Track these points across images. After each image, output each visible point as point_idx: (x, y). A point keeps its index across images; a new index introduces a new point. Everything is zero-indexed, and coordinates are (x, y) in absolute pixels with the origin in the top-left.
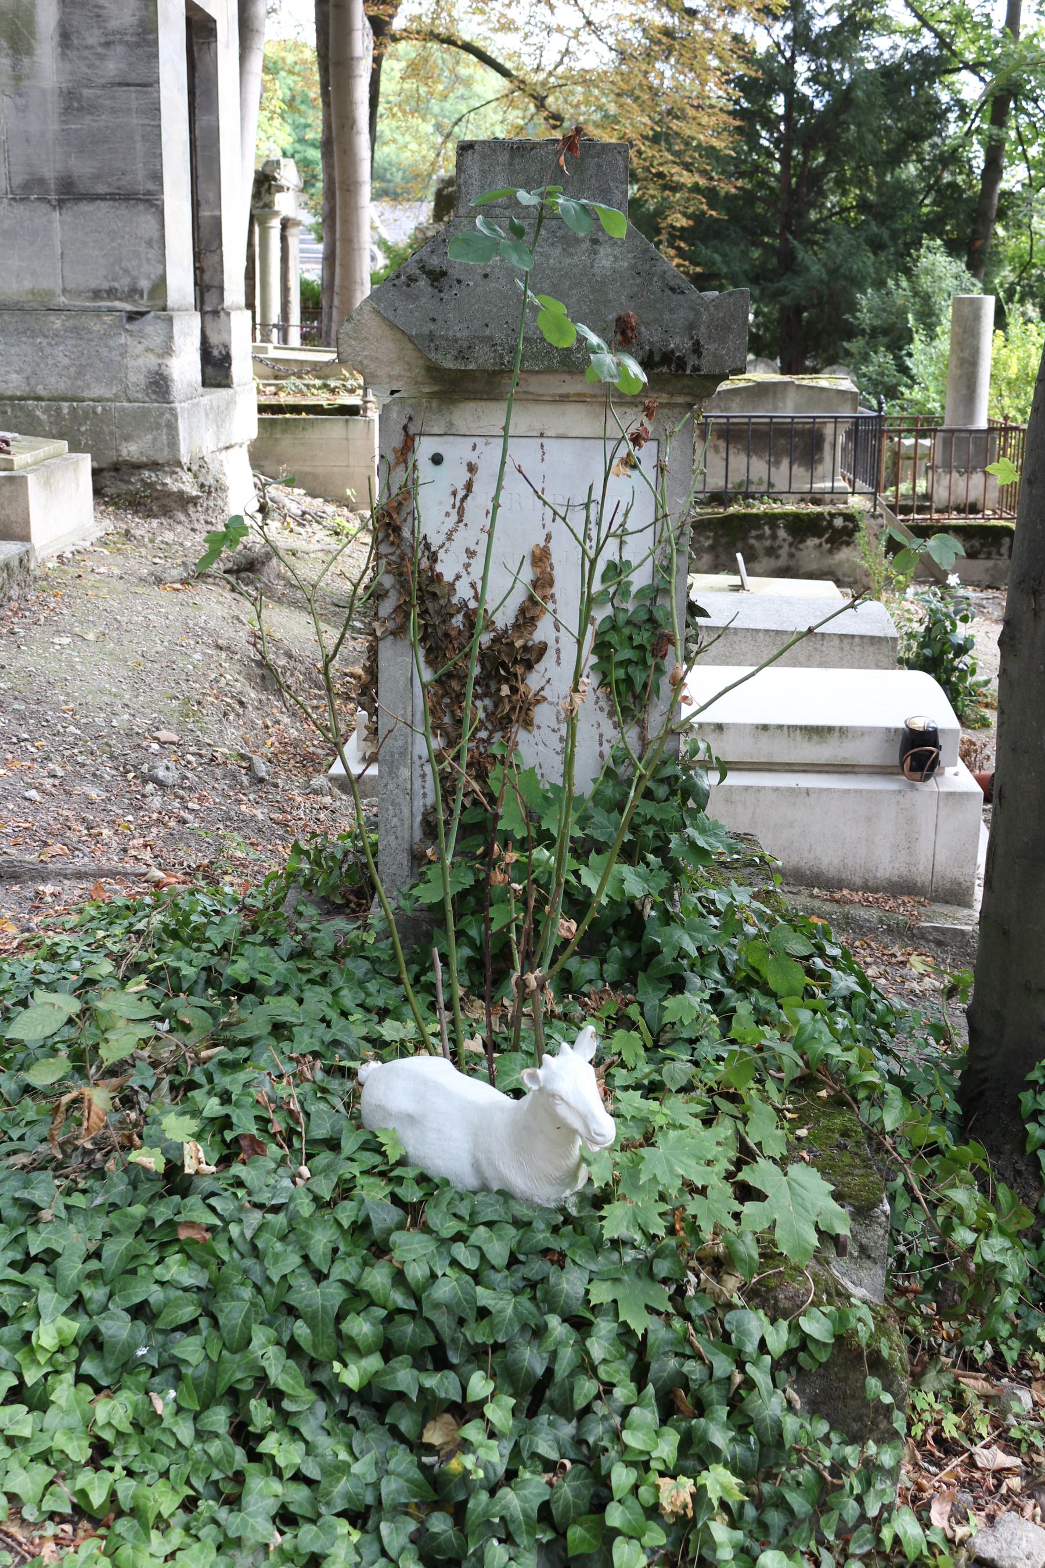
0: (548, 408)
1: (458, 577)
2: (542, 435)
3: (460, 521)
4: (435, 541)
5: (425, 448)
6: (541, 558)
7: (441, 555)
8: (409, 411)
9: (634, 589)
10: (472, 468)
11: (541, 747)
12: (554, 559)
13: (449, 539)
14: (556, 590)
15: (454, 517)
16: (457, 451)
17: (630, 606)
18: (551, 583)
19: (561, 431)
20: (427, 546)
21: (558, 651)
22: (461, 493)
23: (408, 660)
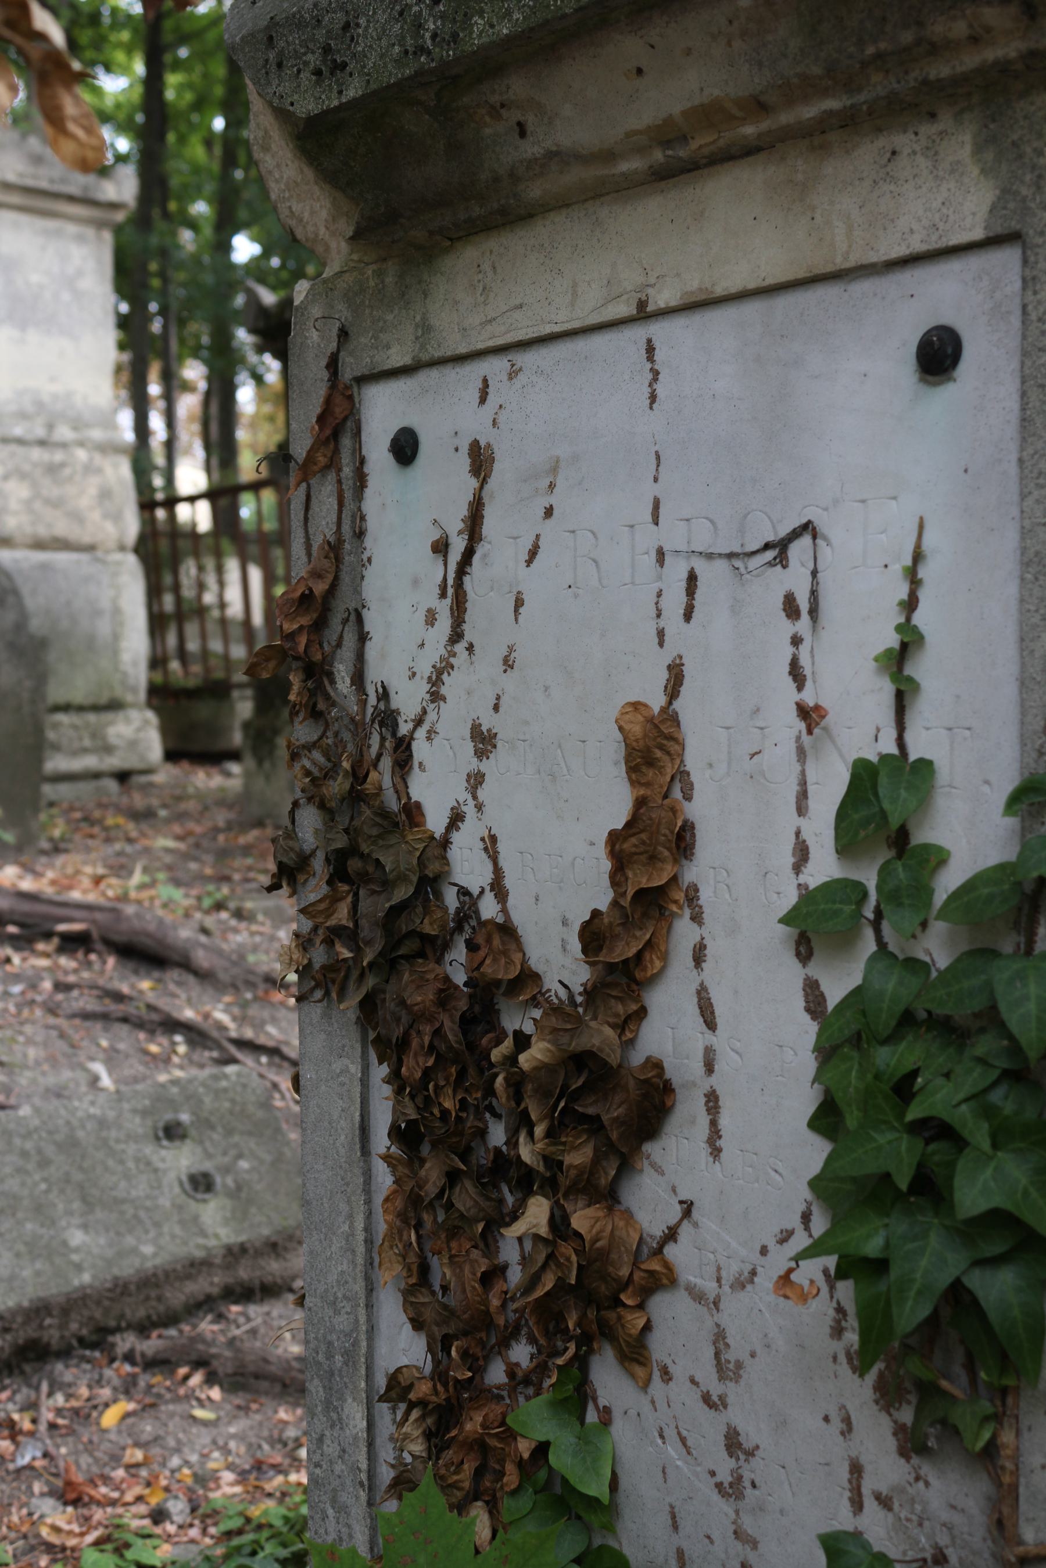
0: (653, 208)
1: (456, 819)
2: (643, 314)
3: (456, 636)
4: (408, 699)
5: (383, 411)
6: (652, 749)
7: (420, 748)
8: (343, 312)
9: (949, 881)
10: (480, 461)
11: (673, 1451)
12: (693, 760)
13: (436, 697)
14: (702, 870)
15: (444, 624)
16: (442, 410)
17: (938, 949)
18: (683, 842)
19: (693, 283)
20: (388, 718)
21: (712, 1100)
22: (458, 546)
23: (355, 1069)
